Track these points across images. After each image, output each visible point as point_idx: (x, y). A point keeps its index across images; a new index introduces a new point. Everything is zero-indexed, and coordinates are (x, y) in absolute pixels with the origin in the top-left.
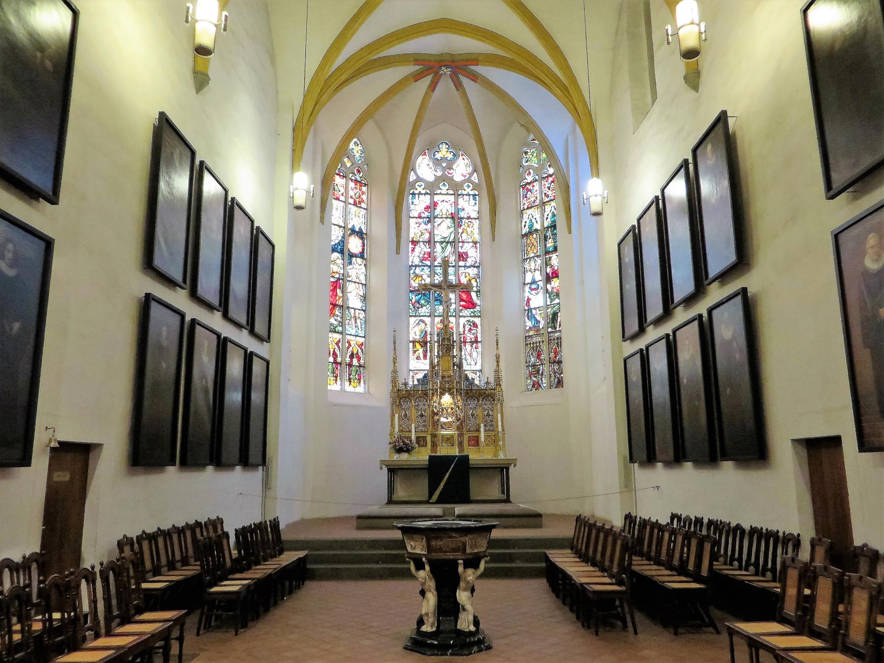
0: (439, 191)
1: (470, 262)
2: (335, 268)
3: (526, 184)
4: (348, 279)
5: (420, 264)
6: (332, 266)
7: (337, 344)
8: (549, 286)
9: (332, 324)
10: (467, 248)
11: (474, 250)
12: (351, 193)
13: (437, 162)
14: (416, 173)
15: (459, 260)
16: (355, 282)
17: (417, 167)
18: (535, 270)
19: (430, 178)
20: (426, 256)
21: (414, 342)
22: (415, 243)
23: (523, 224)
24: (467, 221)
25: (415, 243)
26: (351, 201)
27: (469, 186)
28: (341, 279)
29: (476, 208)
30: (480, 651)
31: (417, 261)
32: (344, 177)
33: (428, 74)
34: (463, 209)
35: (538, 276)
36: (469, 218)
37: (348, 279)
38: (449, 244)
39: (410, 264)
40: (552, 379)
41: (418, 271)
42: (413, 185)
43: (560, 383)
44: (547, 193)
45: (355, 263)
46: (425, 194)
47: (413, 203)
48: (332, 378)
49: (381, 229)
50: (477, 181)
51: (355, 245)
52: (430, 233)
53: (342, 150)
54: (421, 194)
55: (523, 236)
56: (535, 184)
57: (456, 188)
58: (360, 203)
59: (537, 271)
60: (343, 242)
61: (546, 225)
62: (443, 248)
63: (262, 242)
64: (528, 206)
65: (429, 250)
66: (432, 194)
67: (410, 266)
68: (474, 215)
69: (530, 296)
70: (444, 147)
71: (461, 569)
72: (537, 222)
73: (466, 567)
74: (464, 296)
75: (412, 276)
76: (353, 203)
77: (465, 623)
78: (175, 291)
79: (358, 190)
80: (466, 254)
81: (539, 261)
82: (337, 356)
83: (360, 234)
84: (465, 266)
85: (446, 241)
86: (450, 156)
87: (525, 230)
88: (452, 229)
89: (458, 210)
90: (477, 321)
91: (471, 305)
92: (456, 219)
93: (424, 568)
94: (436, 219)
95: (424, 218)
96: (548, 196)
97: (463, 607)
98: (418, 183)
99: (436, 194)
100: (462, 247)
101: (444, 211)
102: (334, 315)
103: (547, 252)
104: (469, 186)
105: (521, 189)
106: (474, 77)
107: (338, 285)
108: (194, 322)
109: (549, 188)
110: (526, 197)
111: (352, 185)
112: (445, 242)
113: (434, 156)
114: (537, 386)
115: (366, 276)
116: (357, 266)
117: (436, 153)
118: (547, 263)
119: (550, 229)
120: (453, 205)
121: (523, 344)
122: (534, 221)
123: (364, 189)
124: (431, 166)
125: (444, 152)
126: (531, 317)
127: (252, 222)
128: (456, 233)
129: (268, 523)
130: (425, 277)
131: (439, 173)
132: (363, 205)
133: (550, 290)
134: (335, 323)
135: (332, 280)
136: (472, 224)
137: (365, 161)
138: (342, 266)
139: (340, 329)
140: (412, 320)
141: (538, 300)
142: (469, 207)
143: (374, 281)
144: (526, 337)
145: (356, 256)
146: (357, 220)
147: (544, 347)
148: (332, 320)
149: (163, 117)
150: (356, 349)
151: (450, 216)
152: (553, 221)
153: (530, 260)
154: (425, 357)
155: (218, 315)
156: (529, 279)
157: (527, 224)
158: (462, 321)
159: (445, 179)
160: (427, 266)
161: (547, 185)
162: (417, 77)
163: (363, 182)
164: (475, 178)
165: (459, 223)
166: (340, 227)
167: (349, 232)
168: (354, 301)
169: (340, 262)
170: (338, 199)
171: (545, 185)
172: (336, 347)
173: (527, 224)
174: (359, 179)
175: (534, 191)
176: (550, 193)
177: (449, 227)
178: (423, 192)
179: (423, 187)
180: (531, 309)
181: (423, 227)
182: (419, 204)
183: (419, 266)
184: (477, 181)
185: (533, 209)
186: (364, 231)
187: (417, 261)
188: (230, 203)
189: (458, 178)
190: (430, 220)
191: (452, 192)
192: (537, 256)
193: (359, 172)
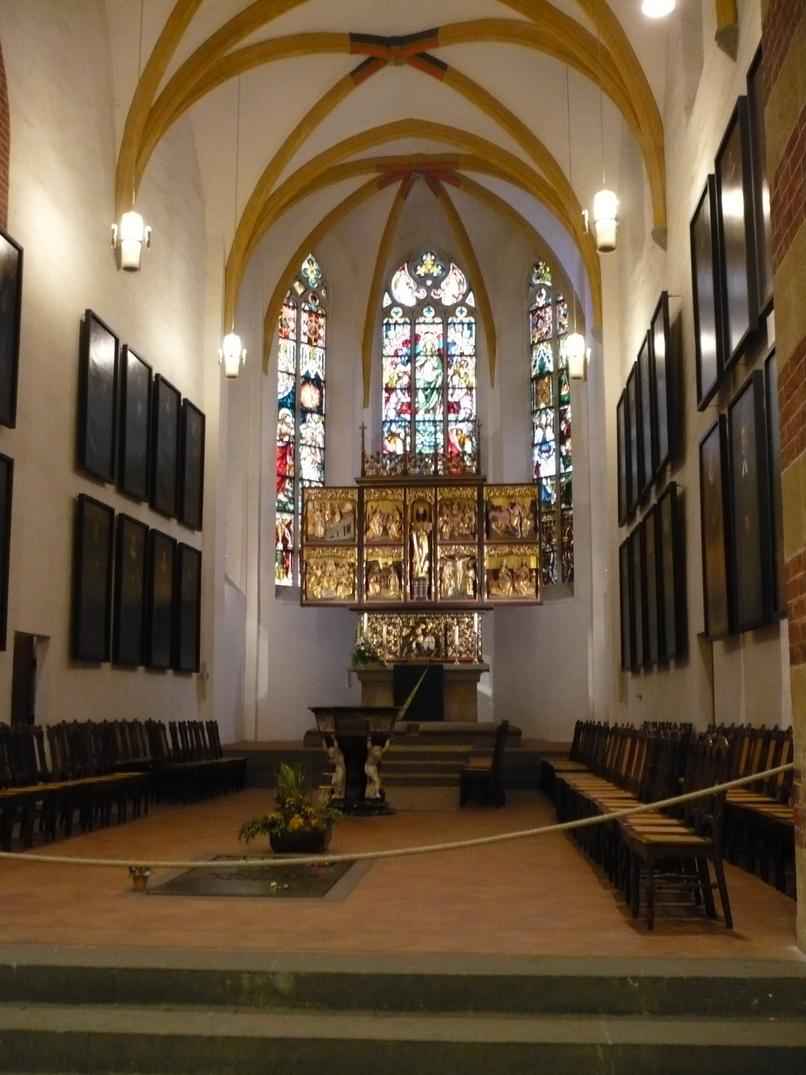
0: (421, 320)
1: (462, 415)
2: (285, 429)
3: (536, 310)
4: (301, 442)
5: (397, 419)
6: (279, 426)
7: (288, 526)
8: (563, 449)
9: (280, 502)
10: (457, 396)
11: (468, 398)
12: (304, 328)
13: (420, 281)
15: (449, 412)
16: (310, 446)
17: (393, 288)
18: (546, 426)
19: (411, 302)
20: (404, 408)
22: (390, 390)
23: (533, 363)
24: (459, 359)
25: (390, 390)
26: (304, 339)
27: (462, 312)
29: (472, 341)
30: (381, 814)
31: (392, 415)
32: (293, 308)
33: (399, 180)
34: (455, 344)
35: (550, 435)
36: (462, 355)
37: (301, 442)
38: (435, 392)
39: (384, 419)
40: (565, 570)
41: (394, 428)
42: (387, 312)
43: (569, 578)
44: (564, 323)
46: (403, 324)
47: (387, 336)
48: (282, 570)
50: (473, 304)
51: (309, 396)
52: (410, 378)
53: (293, 272)
54: (399, 324)
55: (532, 380)
56: (548, 310)
57: (445, 313)
58: (316, 340)
59: (549, 428)
60: (295, 393)
62: (426, 397)
63: (191, 418)
65: (409, 400)
67: (384, 422)
68: (469, 350)
69: (541, 461)
70: (428, 259)
71: (369, 744)
73: (374, 744)
75: (386, 435)
77: (372, 791)
78: (103, 486)
79: (314, 324)
80: (458, 403)
81: (551, 414)
82: (288, 542)
83: (317, 382)
84: (456, 421)
85: (432, 386)
86: (436, 271)
88: (440, 371)
89: (447, 345)
92: (444, 357)
93: (333, 745)
94: (418, 358)
95: (401, 357)
96: (563, 327)
97: (371, 778)
98: (395, 309)
99: (419, 323)
100: (452, 395)
101: (429, 347)
102: (284, 490)
104: (462, 312)
106: (457, 181)
107: (290, 449)
108: (122, 516)
109: (565, 315)
111: (305, 317)
112: (430, 389)
113: (416, 270)
115: (324, 437)
116: (313, 425)
117: (419, 267)
118: (561, 416)
120: (441, 339)
122: (546, 360)
123: (322, 321)
125: (429, 265)
127: (178, 394)
128: (445, 376)
129: (205, 724)
131: (422, 294)
132: (321, 343)
133: (564, 454)
134: (285, 500)
135: (280, 444)
137: (322, 284)
138: (292, 426)
139: (291, 507)
141: (548, 467)
142: (463, 341)
145: (311, 412)
146: (313, 366)
148: (281, 497)
149: (89, 313)
155: (145, 506)
156: (538, 438)
157: (538, 363)
160: (405, 421)
161: (562, 312)
162: (381, 184)
163: (320, 312)
164: (471, 300)
165: (448, 362)
166: (289, 374)
167: (302, 381)
169: (290, 419)
170: (286, 337)
172: (286, 530)
173: (538, 363)
174: (315, 309)
177: (434, 369)
178: (401, 321)
179: (400, 314)
180: (541, 479)
181: (401, 368)
182: (395, 338)
183: (395, 421)
184: (473, 304)
185: (545, 343)
186: (322, 378)
187: (392, 415)
188: (154, 379)
189: (448, 301)
190: (412, 358)
191: (438, 320)
192: (550, 408)
193: (314, 298)
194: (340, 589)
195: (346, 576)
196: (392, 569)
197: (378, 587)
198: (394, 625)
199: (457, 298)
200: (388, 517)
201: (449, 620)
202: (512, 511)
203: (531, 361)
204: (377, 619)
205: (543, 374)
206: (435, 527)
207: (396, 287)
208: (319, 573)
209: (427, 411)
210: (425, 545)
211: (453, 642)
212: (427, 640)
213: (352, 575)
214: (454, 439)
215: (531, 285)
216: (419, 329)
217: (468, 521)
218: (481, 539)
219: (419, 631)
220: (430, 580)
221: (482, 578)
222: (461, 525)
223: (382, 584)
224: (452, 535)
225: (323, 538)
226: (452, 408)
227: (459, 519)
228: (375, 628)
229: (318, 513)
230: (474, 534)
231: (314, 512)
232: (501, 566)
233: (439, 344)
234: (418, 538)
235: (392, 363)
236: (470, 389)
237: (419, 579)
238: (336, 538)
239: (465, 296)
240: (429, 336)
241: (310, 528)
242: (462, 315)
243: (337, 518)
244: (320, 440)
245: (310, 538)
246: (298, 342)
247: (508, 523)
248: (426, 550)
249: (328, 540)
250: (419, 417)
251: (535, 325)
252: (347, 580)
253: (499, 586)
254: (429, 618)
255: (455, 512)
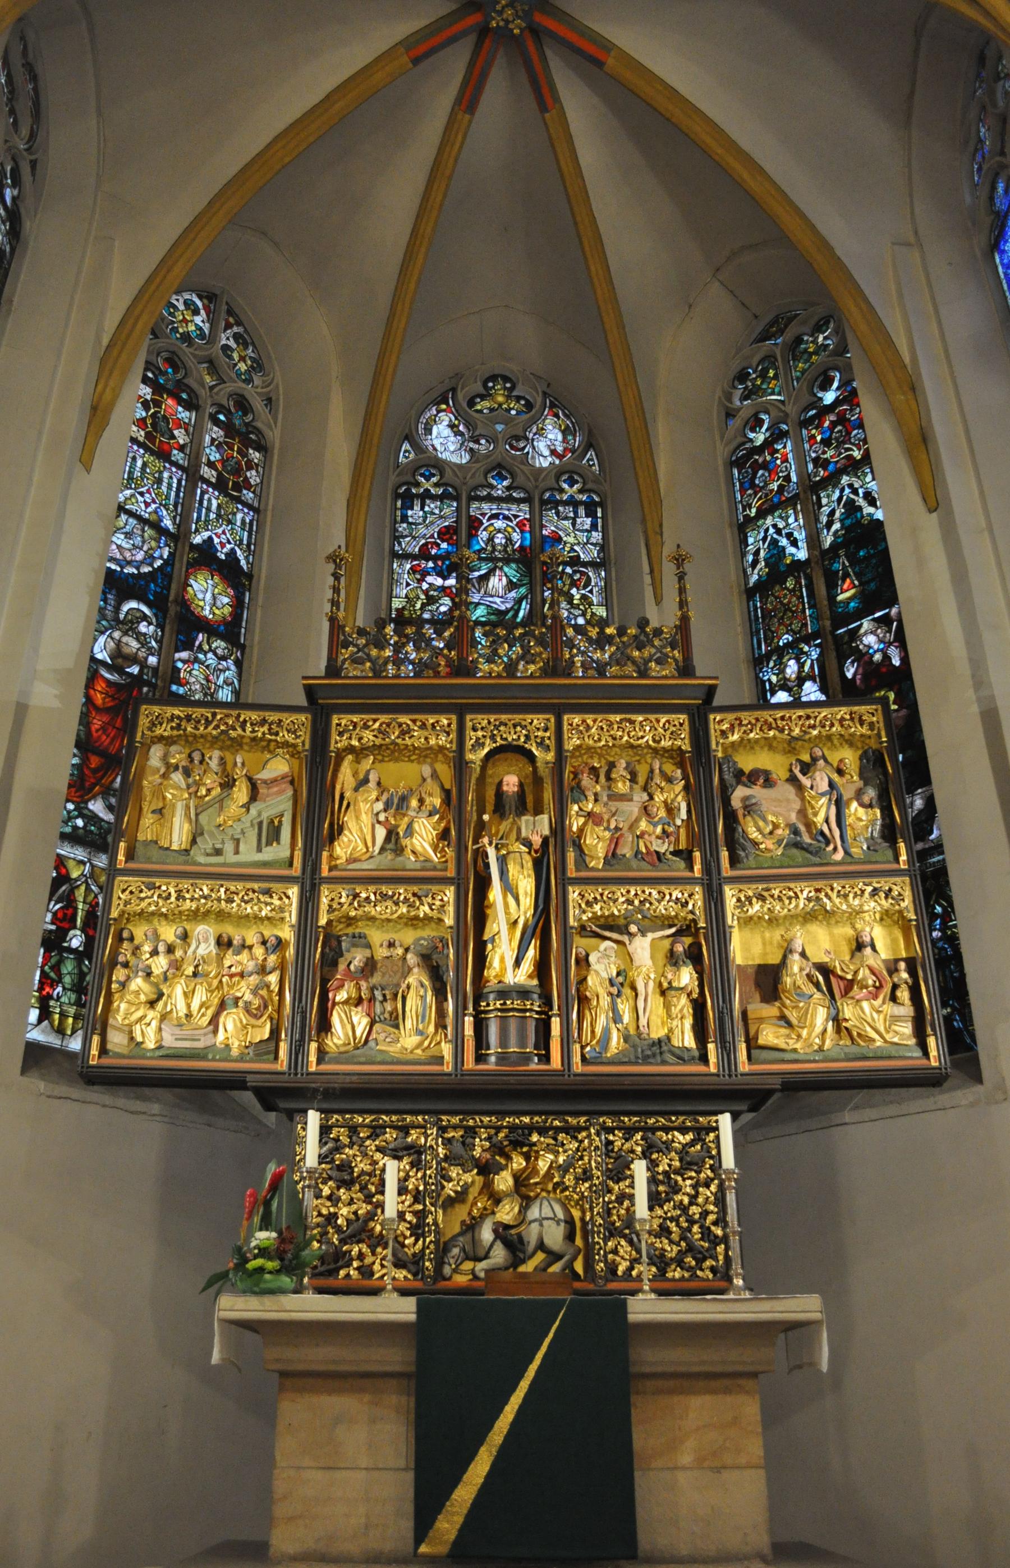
14: (418, 447)
24: (569, 570)
28: (148, 684)
29: (596, 536)
36: (575, 561)
37: (174, 688)
45: (206, 647)
46: (441, 498)
47: (404, 519)
54: (434, 498)
55: (750, 593)
58: (237, 487)
61: (828, 541)
64: (759, 509)
72: (794, 543)
76: (213, 480)
95: (435, 558)
101: (499, 539)
105: (736, 472)
110: (753, 485)
116: (211, 659)
119: (842, 552)
120: (527, 528)
122: (784, 542)
124: (461, 428)
136: (584, 578)
151: (517, 555)
152: (852, 525)
153: (781, 657)
171: (813, 437)
173: (762, 554)
175: (778, 462)
179: (434, 480)
192: (808, 639)
194: (231, 1022)
195: (254, 980)
196: (412, 959)
197: (361, 1021)
198: (415, 1153)
199: (560, 457)
200: (404, 799)
201: (617, 1139)
202: (806, 781)
203: (743, 554)
204: (353, 1130)
206: (559, 829)
207: (428, 431)
208: (160, 964)
210: (526, 884)
211: (630, 1219)
212: (534, 1213)
213: (273, 979)
217: (662, 813)
218: (711, 867)
219: (504, 1181)
220: (547, 1000)
221: (728, 999)
222: (643, 825)
223: (378, 1009)
224: (612, 857)
225: (187, 851)
227: (633, 809)
228: (346, 1167)
229: (177, 777)
230: (686, 856)
231: (165, 776)
232: (788, 951)
234: (503, 861)
235: (413, 570)
237: (504, 993)
238: (230, 857)
240: (499, 524)
241: (148, 820)
243: (241, 793)
245: (140, 850)
246: (192, 474)
247: (793, 817)
248: (527, 902)
249: (202, 859)
252: (255, 992)
253: (783, 1017)
254: (542, 1131)
255: (622, 787)
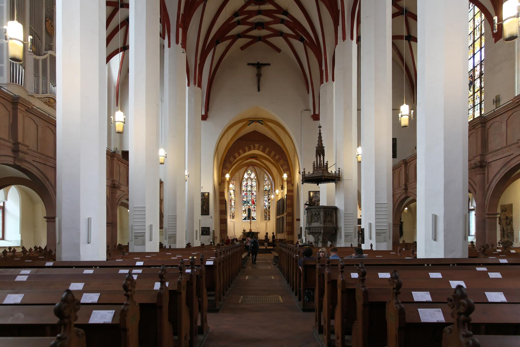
1: (254, 195)
10: (254, 192)
13: (248, 174)
19: (247, 178)
21: (243, 211)
22: (244, 191)
25: (244, 191)
29: (256, 184)
31: (244, 195)
35: (267, 199)
41: (244, 197)
49: (238, 190)
57: (252, 179)
66: (247, 181)
68: (255, 185)
70: (249, 171)
74: (253, 202)
81: (267, 196)
86: (250, 173)
87: (265, 190)
89: (252, 184)
90: (255, 207)
91: (254, 203)
92: (251, 186)
103: (269, 195)
112: (249, 191)
114: (266, 219)
121: (264, 212)
123: (234, 181)
125: (249, 172)
126: (265, 207)
128: (252, 189)
130: (245, 198)
131: (248, 177)
132: (234, 185)
140: (243, 206)
142: (254, 184)
143: (236, 200)
144: (264, 210)
147: (268, 212)
150: (233, 213)
154: (245, 214)
158: (253, 207)
159: (249, 178)
164: (255, 178)
168: (233, 204)
176: (269, 183)
181: (245, 188)
182: (244, 183)
187: (244, 195)
189: (252, 178)
190: (247, 186)
205: (266, 190)
209: (249, 194)
214: (253, 199)
215: (264, 176)
216: (248, 182)
226: (253, 194)
233: (251, 184)
236: (255, 191)
239: (255, 177)
242: (254, 180)
244: (234, 199)
250: (248, 195)
251: (265, 183)
